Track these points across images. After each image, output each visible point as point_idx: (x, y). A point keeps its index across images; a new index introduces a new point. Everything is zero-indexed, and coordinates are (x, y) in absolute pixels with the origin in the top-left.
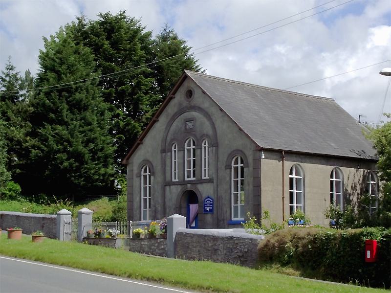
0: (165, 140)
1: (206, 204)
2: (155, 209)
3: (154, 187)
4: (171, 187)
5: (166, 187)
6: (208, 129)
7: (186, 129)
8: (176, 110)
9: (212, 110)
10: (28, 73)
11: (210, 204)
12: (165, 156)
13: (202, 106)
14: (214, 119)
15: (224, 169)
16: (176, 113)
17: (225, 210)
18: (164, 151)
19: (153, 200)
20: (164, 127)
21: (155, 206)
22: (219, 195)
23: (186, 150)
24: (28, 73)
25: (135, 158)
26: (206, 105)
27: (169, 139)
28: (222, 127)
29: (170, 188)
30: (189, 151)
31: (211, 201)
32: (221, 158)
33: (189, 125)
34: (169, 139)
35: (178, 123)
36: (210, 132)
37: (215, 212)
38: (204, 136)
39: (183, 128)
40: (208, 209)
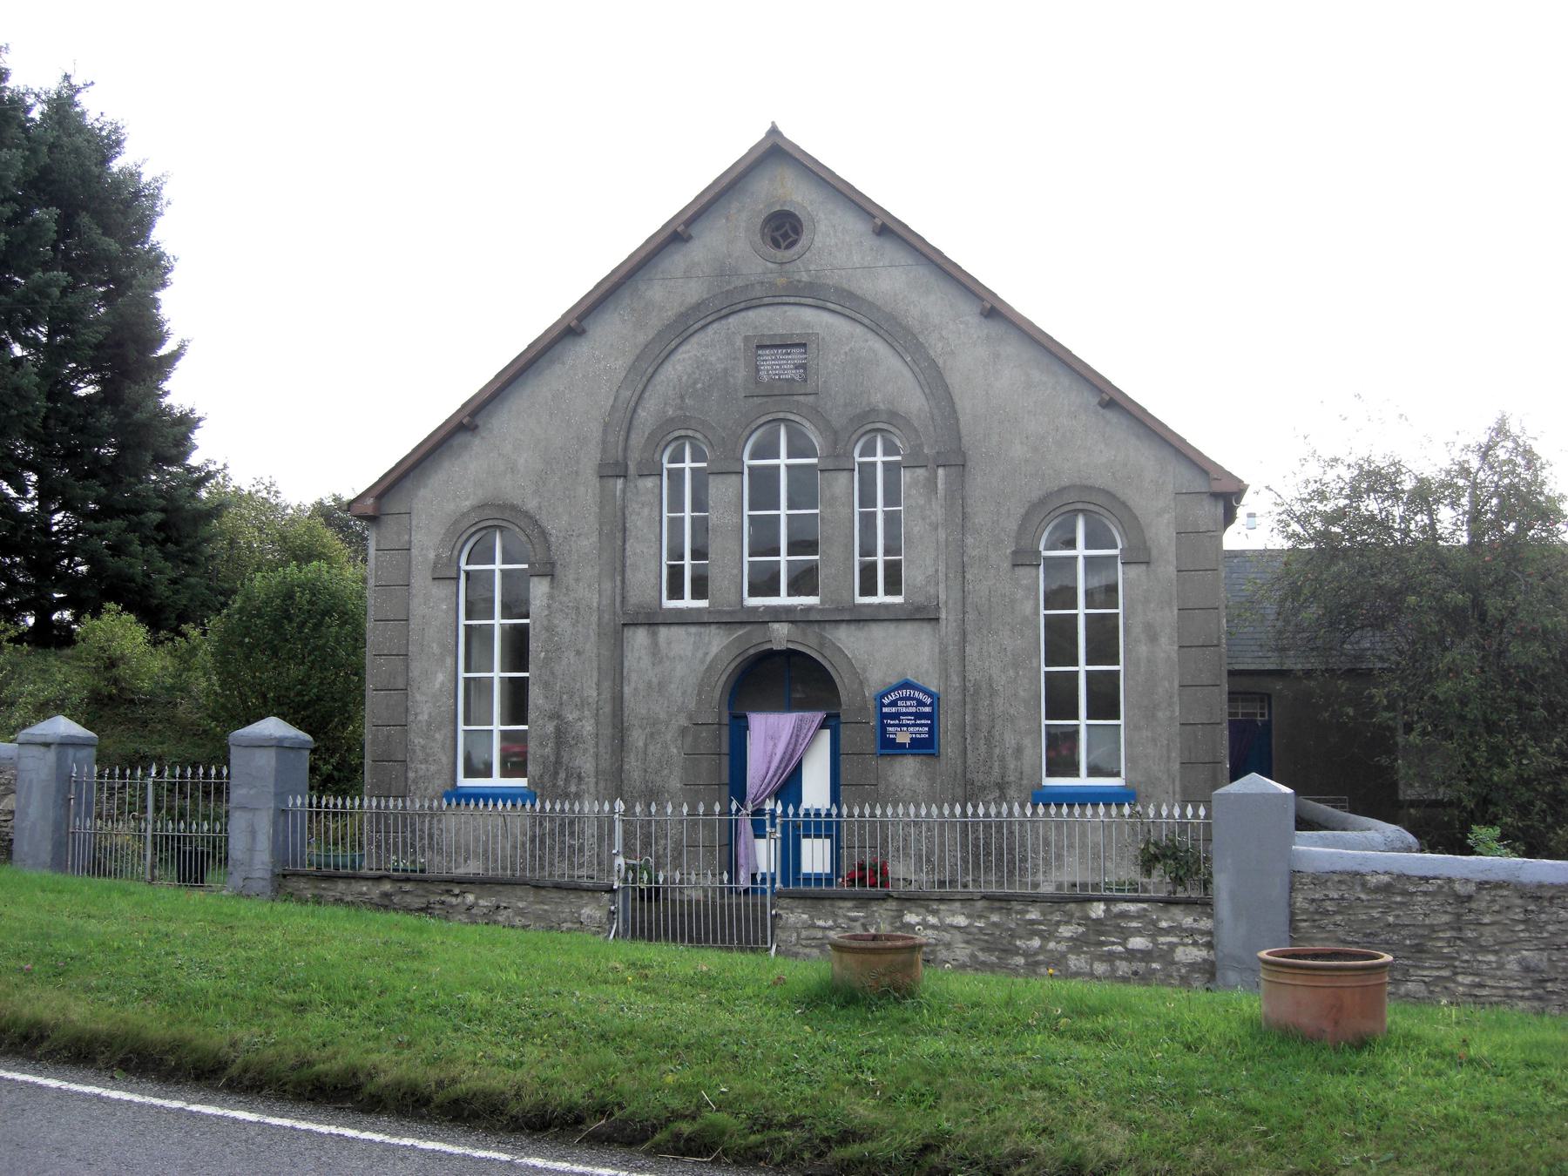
0: (624, 418)
1: (896, 716)
2: (557, 729)
3: (550, 629)
4: (663, 632)
5: (628, 632)
6: (892, 381)
7: (758, 382)
8: (694, 292)
9: (928, 306)
10: (166, 393)
11: (918, 716)
12: (624, 491)
13: (865, 286)
14: (936, 348)
15: (1006, 565)
16: (697, 307)
17: (1010, 739)
18: (613, 469)
19: (547, 685)
20: (620, 364)
21: (556, 716)
22: (970, 677)
23: (746, 471)
24: (166, 393)
25: (422, 492)
26: (890, 281)
27: (647, 415)
28: (981, 375)
29: (654, 634)
30: (676, 476)
31: (923, 704)
32: (981, 515)
33: (776, 366)
34: (647, 415)
35: (707, 351)
36: (914, 401)
37: (949, 745)
38: (871, 423)
39: (741, 374)
40: (903, 738)
